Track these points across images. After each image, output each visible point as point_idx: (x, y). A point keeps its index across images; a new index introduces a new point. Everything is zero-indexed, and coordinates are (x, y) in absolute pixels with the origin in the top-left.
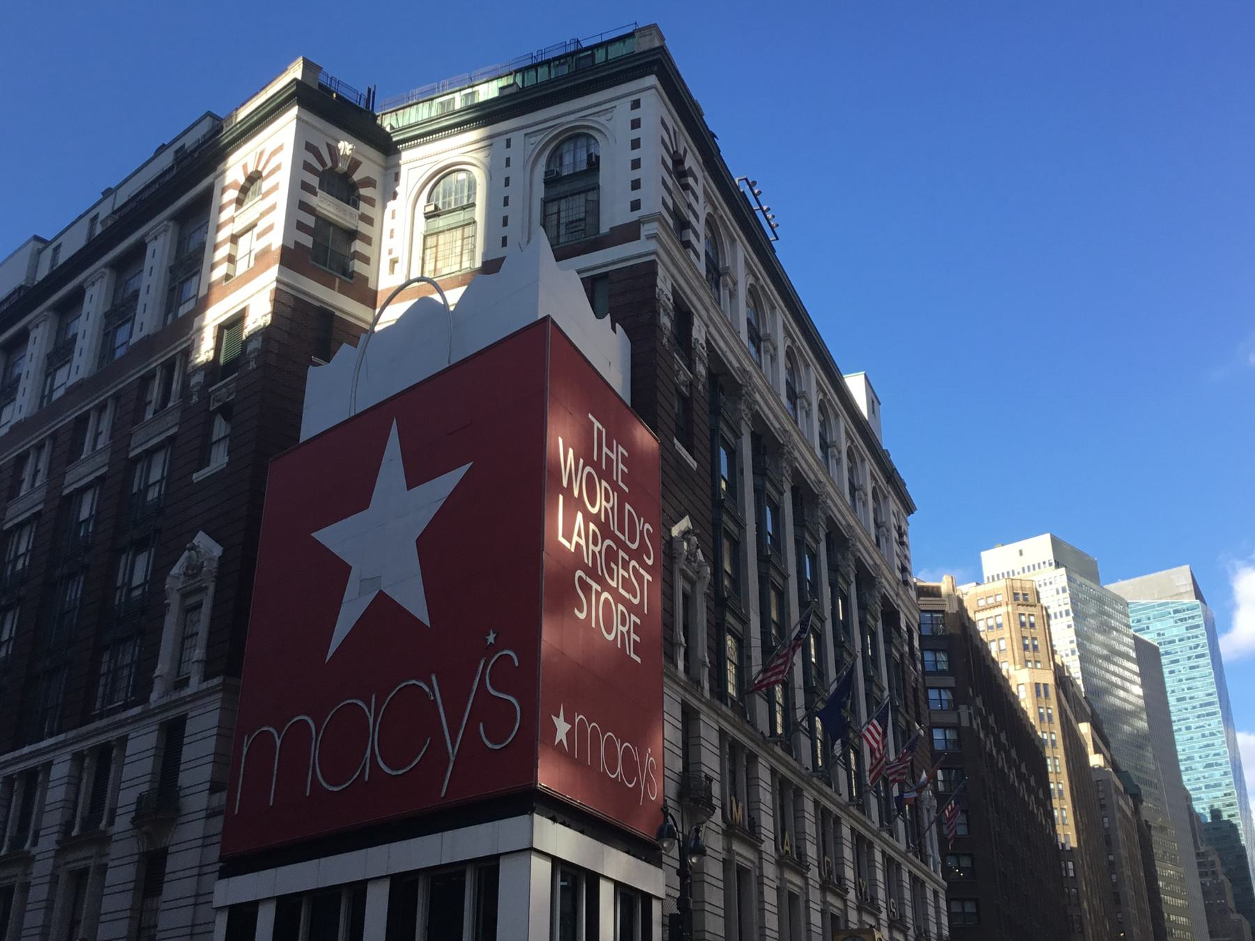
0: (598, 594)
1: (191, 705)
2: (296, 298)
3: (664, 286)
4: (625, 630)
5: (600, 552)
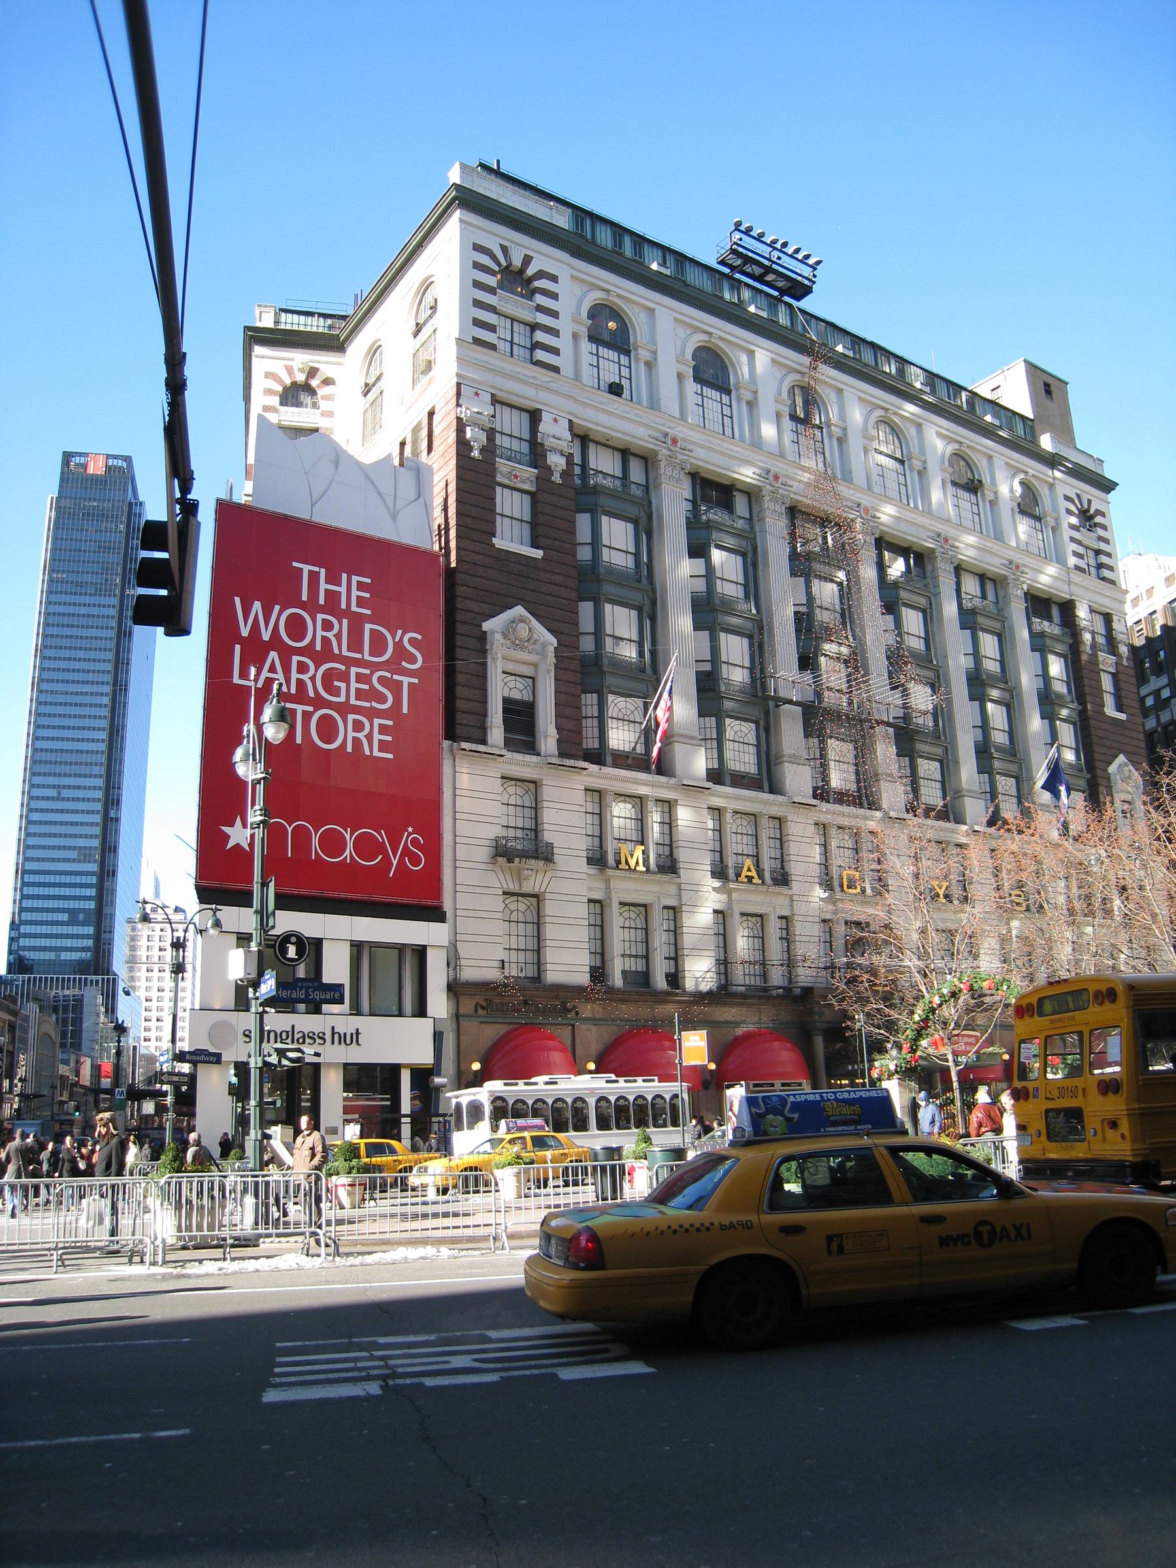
0: (307, 716)
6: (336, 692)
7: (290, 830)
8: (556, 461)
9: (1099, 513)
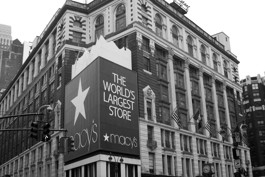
0: (117, 110)
1: (59, 134)
2: (70, 50)
3: (139, 37)
4: (126, 115)
5: (117, 101)
6: (121, 104)
7: (115, 137)
8: (153, 51)
9: (237, 69)
